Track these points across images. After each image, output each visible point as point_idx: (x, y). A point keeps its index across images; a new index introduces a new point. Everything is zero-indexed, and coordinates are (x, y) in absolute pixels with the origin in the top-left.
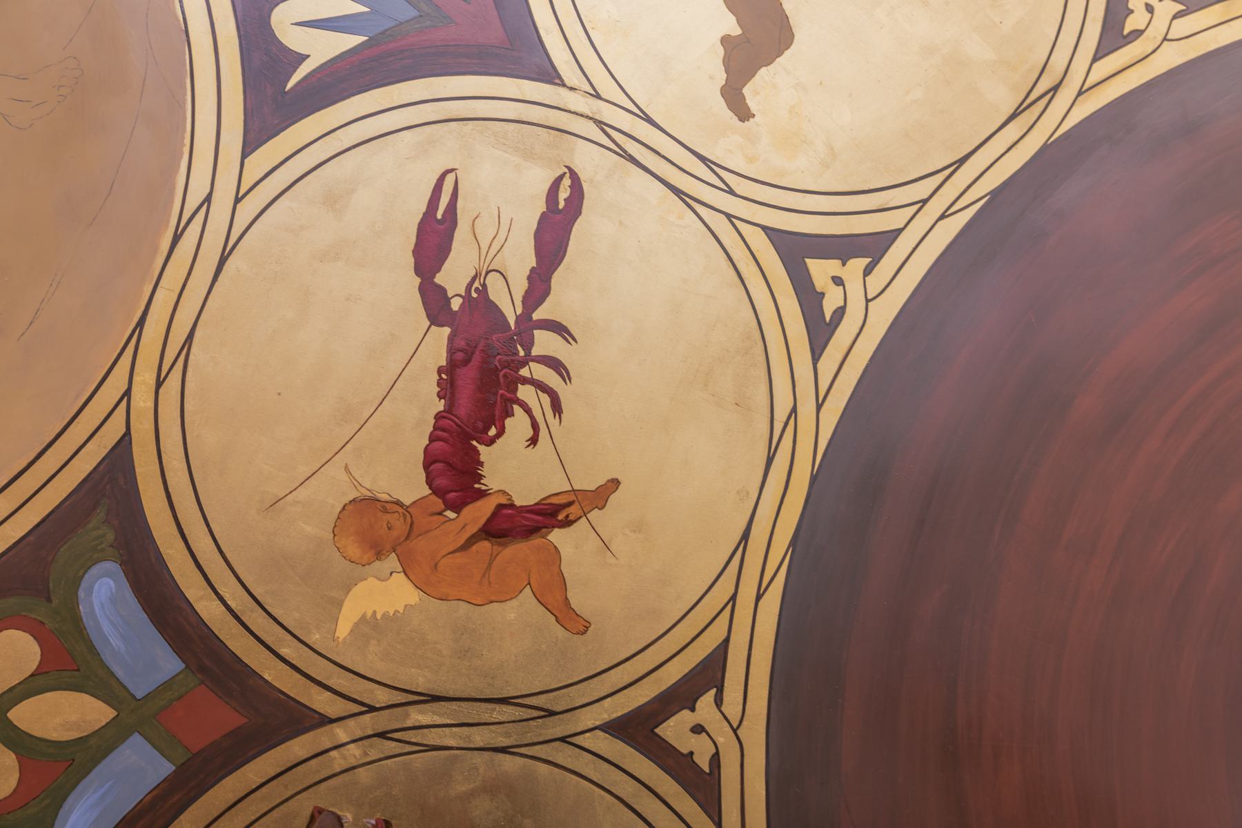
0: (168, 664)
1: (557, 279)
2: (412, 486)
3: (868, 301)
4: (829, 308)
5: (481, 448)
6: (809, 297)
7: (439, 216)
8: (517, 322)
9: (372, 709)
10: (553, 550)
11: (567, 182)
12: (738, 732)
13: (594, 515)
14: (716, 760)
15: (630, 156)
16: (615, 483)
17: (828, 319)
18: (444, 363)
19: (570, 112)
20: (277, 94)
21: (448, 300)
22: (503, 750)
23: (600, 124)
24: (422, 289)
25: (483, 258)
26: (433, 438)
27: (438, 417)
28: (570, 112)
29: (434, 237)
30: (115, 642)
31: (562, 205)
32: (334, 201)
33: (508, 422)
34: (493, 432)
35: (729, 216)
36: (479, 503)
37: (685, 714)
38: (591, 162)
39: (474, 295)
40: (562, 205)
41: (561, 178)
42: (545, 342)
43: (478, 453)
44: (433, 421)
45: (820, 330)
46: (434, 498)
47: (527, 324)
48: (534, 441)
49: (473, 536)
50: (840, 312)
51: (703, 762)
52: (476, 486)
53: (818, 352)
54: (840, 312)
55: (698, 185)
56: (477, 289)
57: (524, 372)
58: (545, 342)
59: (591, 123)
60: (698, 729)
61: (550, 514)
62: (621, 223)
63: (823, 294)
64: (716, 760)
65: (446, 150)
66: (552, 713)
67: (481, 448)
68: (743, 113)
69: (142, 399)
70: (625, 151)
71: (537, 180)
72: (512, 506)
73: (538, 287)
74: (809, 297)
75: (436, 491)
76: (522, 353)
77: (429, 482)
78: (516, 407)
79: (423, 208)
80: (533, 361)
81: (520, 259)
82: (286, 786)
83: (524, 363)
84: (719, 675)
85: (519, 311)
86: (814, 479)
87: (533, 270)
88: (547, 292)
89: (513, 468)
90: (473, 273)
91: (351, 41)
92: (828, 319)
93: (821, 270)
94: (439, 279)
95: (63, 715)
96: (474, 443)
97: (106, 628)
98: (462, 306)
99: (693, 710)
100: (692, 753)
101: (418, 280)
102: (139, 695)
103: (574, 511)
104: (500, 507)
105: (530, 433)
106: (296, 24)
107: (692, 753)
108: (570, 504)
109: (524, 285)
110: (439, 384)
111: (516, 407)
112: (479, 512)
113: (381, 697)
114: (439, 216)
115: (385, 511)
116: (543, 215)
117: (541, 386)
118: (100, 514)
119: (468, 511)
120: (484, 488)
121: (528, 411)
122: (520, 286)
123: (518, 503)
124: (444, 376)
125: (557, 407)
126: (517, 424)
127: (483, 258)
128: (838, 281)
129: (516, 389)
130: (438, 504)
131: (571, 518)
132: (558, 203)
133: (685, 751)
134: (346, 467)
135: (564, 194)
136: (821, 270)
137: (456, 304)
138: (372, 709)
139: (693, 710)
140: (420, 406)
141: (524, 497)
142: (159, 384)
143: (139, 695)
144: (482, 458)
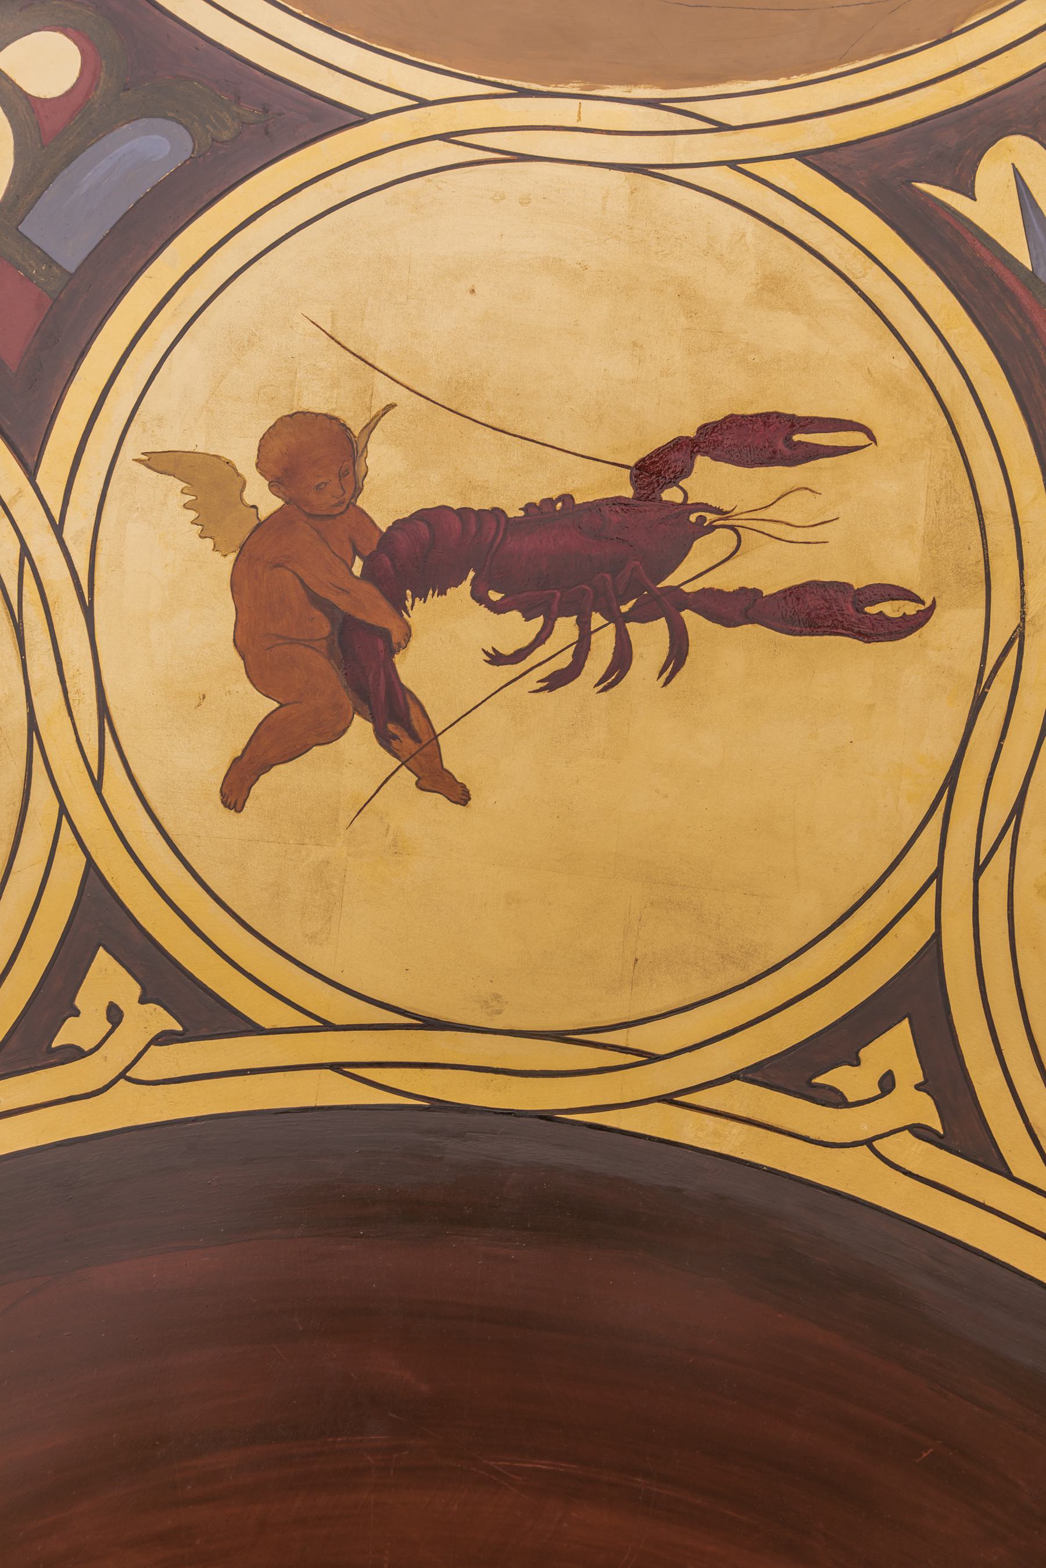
0: (71, 255)
1: (753, 633)
3: (869, 1143)
4: (836, 1078)
5: (466, 586)
6: (846, 1039)
7: (796, 438)
8: (670, 588)
10: (340, 728)
11: (911, 608)
12: (122, 1081)
13: (407, 778)
14: (74, 1053)
15: (984, 694)
16: (460, 795)
17: (818, 1080)
18: (578, 501)
19: (1022, 586)
21: (674, 482)
24: (678, 444)
25: (753, 515)
26: (464, 512)
27: (497, 513)
28: (1022, 586)
29: (765, 438)
32: (773, 288)
33: (515, 615)
34: (495, 596)
35: (937, 875)
36: (384, 604)
37: (135, 989)
38: (955, 635)
39: (693, 518)
41: (917, 600)
42: (650, 639)
44: (487, 507)
45: (795, 1072)
46: (376, 540)
47: (670, 606)
48: (496, 659)
49: (334, 606)
50: (835, 1099)
51: (67, 1035)
52: (408, 592)
54: (835, 1099)
56: (702, 519)
57: (597, 620)
58: (650, 639)
59: (1016, 622)
60: (115, 1015)
62: (871, 707)
63: (858, 1064)
64: (74, 1053)
65: (904, 423)
66: (98, 784)
67: (466, 586)
70: (988, 685)
71: (899, 563)
72: (391, 651)
73: (735, 608)
74: (846, 1039)
76: (624, 609)
77: (398, 525)
78: (540, 620)
79: (801, 412)
81: (768, 569)
85: (687, 588)
86: (547, 1117)
87: (757, 592)
88: (729, 622)
89: (448, 641)
90: (726, 508)
92: (818, 1080)
93: (895, 1048)
94: (702, 463)
96: (472, 574)
98: (673, 504)
99: (143, 1001)
100: (77, 1013)
101: (691, 433)
103: (408, 744)
105: (507, 650)
107: (77, 1013)
108: (415, 737)
110: (543, 501)
111: (540, 620)
114: (796, 438)
115: (341, 475)
117: (582, 649)
119: (369, 590)
120: (408, 604)
121: (541, 639)
122: (726, 580)
123: (397, 658)
124: (559, 505)
125: (556, 681)
126: (515, 629)
127: (753, 515)
128: (887, 1083)
129: (568, 615)
130: (370, 546)
131: (395, 744)
133: (78, 1002)
134: (392, 406)
135: (891, 609)
136: (895, 1048)
137: (671, 495)
139: (143, 1001)
140: (507, 483)
141: (410, 668)
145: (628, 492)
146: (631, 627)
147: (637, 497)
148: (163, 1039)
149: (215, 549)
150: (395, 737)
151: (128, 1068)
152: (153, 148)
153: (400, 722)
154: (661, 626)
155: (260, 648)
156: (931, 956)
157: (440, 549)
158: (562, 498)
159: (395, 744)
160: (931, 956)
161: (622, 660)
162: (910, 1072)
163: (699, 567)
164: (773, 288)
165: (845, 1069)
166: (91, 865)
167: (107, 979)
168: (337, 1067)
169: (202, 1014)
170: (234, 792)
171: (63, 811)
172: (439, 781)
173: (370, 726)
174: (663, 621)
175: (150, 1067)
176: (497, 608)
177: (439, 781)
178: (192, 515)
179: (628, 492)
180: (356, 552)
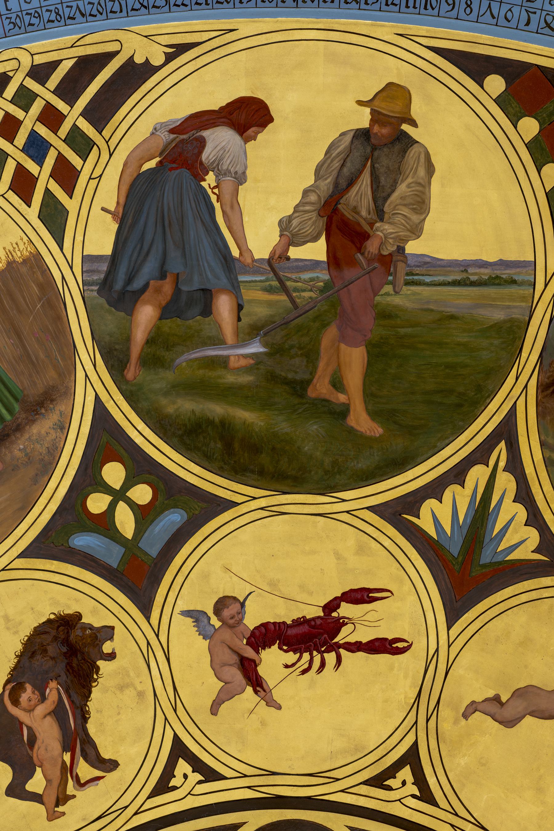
0: (154, 552)
1: (361, 654)
2: (252, 620)
3: (399, 800)
5: (277, 645)
7: (370, 595)
9: (157, 636)
11: (406, 644)
13: (263, 703)
14: (175, 788)
16: (279, 707)
17: (385, 783)
18: (307, 618)
20: (399, 513)
21: (335, 610)
22: (155, 695)
23: (437, 650)
24: (336, 598)
26: (274, 623)
27: (284, 623)
29: (361, 596)
30: (157, 529)
31: (394, 646)
33: (291, 653)
34: (285, 648)
39: (341, 621)
40: (394, 646)
42: (330, 658)
43: (274, 644)
44: (281, 621)
47: (335, 648)
48: (287, 666)
50: (389, 788)
51: (173, 783)
53: (368, 783)
54: (389, 788)
55: (425, 704)
56: (344, 621)
57: (315, 653)
60: (185, 776)
61: (257, 683)
63: (395, 778)
64: (175, 788)
66: (175, 711)
67: (277, 645)
68: (465, 716)
69: (254, 504)
72: (256, 666)
73: (355, 647)
75: (253, 633)
76: (323, 649)
77: (256, 628)
78: (298, 655)
80: (321, 656)
81: (364, 635)
82: (119, 612)
83: (319, 652)
84: (211, 779)
85: (341, 642)
86: (309, 798)
87: (361, 642)
88: (353, 651)
89: (273, 661)
91: (432, 532)
92: (385, 783)
93: (406, 773)
94: (343, 604)
95: (125, 521)
96: (278, 642)
97: (162, 524)
99: (193, 772)
100: (175, 777)
101: (340, 595)
103: (262, 693)
104: (254, 661)
105: (289, 664)
106: (432, 510)
107: (175, 777)
108: (264, 691)
109: (353, 641)
110: (298, 618)
111: (298, 655)
112: (249, 653)
114: (370, 595)
116: (386, 639)
118: (204, 505)
120: (260, 652)
122: (352, 639)
123: (258, 668)
125: (304, 672)
126: (291, 657)
128: (404, 783)
130: (248, 635)
131: (259, 693)
132: (394, 644)
133: (175, 773)
136: (406, 773)
137: (334, 614)
138: (157, 636)
139: (193, 772)
141: (261, 670)
142: (262, 509)
144: (272, 647)
145: (322, 614)
146: (325, 655)
147: (325, 615)
148: (200, 782)
149: (204, 638)
150: (259, 691)
151: (191, 791)
154: (333, 654)
156: (415, 746)
157: (268, 635)
158: (303, 617)
159: (259, 693)
160: (415, 746)
161: (323, 665)
162: (410, 779)
163: (345, 635)
164: (361, 550)
165: (392, 780)
167: (183, 767)
168: (249, 787)
170: (214, 709)
172: (272, 703)
173: (252, 688)
174: (334, 653)
176: (286, 651)
177: (272, 703)
178: (196, 629)
179: (322, 614)
180: (244, 637)
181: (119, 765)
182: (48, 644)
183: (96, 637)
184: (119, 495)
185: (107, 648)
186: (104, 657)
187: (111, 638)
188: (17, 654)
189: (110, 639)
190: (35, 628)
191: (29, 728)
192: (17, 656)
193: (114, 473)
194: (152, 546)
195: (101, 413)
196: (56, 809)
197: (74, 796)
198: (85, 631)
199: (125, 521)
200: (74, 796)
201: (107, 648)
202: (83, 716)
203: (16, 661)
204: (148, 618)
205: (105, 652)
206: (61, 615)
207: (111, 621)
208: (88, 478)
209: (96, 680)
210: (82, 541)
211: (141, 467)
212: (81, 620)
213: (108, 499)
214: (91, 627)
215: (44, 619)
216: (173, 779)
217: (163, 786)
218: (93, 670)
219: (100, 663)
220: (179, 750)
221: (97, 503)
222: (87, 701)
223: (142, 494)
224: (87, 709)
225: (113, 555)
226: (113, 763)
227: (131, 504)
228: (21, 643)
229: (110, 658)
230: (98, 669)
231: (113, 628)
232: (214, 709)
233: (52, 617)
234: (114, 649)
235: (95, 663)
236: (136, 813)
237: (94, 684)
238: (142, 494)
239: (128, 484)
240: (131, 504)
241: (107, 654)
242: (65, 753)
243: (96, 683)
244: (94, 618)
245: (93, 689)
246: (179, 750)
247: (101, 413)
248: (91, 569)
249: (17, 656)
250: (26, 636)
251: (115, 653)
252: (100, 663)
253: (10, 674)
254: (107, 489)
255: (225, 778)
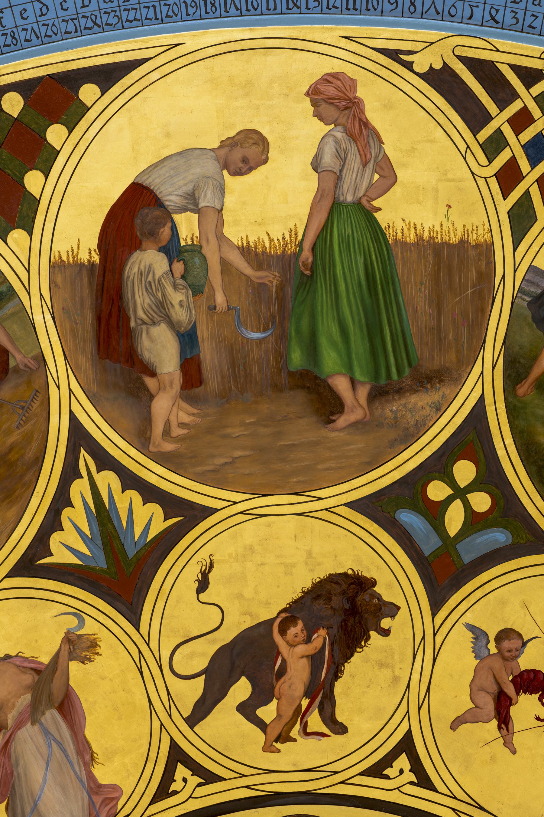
0: (467, 559)
5: (538, 695)
9: (435, 635)
13: (501, 740)
14: (387, 777)
16: (514, 752)
22: (408, 686)
30: (480, 540)
37: (409, 767)
48: (538, 719)
51: (387, 772)
60: (401, 772)
64: (387, 777)
66: (419, 708)
67: (538, 695)
72: (511, 705)
77: (526, 671)
95: (454, 519)
96: (540, 693)
97: (486, 537)
99: (410, 771)
100: (392, 767)
102: (457, 546)
103: (505, 732)
104: (511, 700)
107: (392, 767)
108: (508, 730)
113: (439, 639)
118: (532, 538)
120: (520, 694)
123: (511, 708)
130: (516, 673)
131: (502, 730)
133: (393, 764)
138: (435, 635)
139: (410, 771)
141: (514, 711)
143: (457, 546)
148: (412, 783)
149: (475, 657)
150: (503, 728)
152: (499, 537)
153: (504, 721)
155: (475, 688)
159: (502, 730)
166: (410, 730)
167: (403, 762)
169: (424, 781)
170: (455, 725)
171: (408, 712)
173: (497, 723)
175: (405, 789)
178: (473, 645)
180: (512, 674)
181: (348, 732)
182: (335, 595)
183: (380, 609)
184: (460, 493)
185: (385, 623)
186: (379, 630)
187: (393, 616)
188: (304, 590)
189: (391, 617)
190: (330, 575)
191: (284, 661)
192: (303, 592)
193: (465, 471)
194: (468, 553)
195: (479, 412)
196: (274, 744)
197: (295, 740)
198: (373, 599)
199: (454, 519)
200: (295, 740)
201: (385, 623)
202: (336, 673)
203: (300, 595)
204: (434, 615)
205: (382, 626)
206: (358, 574)
207: (399, 601)
208: (439, 465)
209: (362, 647)
210: (408, 518)
211: (491, 477)
212: (374, 587)
213: (449, 491)
214: (379, 598)
215: (341, 571)
216: (390, 768)
217: (377, 771)
218: (364, 637)
219: (373, 633)
220: (406, 745)
221: (437, 491)
222: (346, 662)
223: (481, 502)
224: (343, 669)
225: (429, 544)
226: (343, 728)
227: (467, 505)
228: (312, 582)
229: (383, 634)
230: (369, 638)
231: (398, 608)
232: (455, 725)
233: (350, 572)
234: (390, 627)
235: (369, 632)
236: (342, 782)
237: (359, 650)
238: (481, 502)
239: (472, 487)
240: (467, 505)
241: (383, 628)
242: (305, 698)
243: (361, 650)
244: (386, 591)
245: (356, 654)
246: (406, 745)
247: (479, 412)
248: (404, 546)
249: (303, 592)
250: (319, 578)
251: (390, 631)
252: (373, 633)
253: (289, 604)
254: (452, 482)
255: (436, 791)
